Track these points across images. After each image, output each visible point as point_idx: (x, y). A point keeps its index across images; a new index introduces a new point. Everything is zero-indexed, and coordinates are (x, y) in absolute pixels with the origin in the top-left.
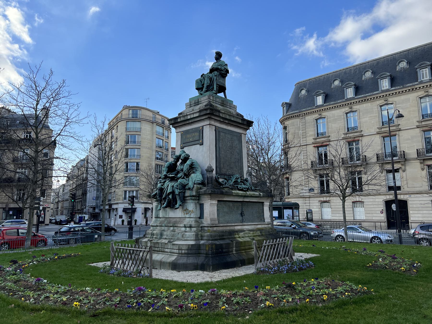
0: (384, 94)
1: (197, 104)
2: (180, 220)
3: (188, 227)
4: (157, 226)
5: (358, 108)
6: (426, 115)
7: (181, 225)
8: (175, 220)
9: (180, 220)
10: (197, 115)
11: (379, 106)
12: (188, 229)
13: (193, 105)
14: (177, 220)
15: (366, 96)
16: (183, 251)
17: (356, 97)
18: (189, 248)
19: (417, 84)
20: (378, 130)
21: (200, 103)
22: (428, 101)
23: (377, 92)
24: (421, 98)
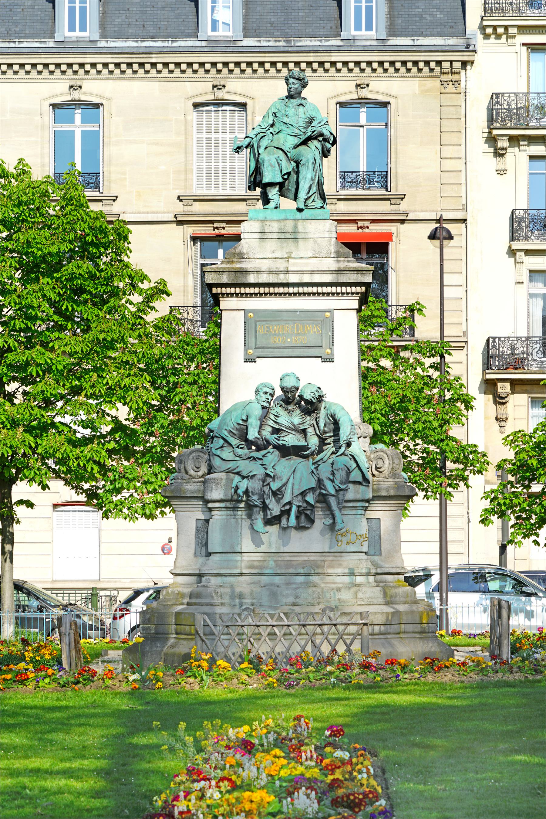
0: (219, 58)
1: (288, 235)
2: (335, 558)
3: (361, 575)
4: (241, 574)
5: (107, 95)
6: (353, 177)
7: (339, 571)
8: (306, 558)
9: (323, 558)
10: (327, 278)
11: (191, 103)
12: (359, 579)
13: (275, 235)
14: (312, 558)
15: (148, 52)
16: (376, 629)
17: (103, 44)
18: (387, 619)
19: (339, 50)
20: (179, 208)
21: (300, 235)
22: (363, 121)
23: (190, 42)
24: (342, 105)
